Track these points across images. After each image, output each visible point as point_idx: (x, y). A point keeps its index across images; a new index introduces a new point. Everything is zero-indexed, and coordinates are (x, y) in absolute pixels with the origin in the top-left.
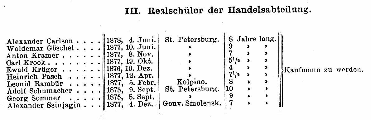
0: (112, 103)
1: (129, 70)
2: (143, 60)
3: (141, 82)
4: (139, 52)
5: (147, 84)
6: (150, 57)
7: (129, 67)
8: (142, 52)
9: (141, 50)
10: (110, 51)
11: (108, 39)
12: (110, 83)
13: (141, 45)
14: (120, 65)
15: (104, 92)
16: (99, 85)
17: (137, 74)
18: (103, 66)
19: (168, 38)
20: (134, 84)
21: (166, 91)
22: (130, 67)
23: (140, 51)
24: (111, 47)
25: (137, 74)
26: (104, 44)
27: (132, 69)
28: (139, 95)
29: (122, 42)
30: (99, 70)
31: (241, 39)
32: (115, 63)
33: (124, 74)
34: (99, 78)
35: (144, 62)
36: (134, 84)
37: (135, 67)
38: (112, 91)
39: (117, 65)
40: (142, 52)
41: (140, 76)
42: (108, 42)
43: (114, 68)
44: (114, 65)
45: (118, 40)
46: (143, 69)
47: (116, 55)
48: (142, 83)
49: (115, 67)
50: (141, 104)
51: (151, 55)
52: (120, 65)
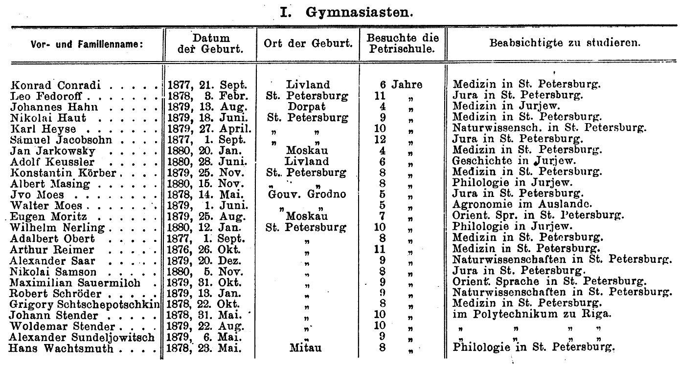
0: (175, 259)
1: (205, 295)
2: (227, 280)
3: (224, 95)
4: (222, 169)
5: (235, 98)
6: (239, 277)
7: (206, 104)
8: (226, 169)
9: (225, 166)
10: (172, 244)
11: (170, 82)
12: (171, 250)
13: (225, 115)
14: (189, 144)
15: (162, 265)
16: (156, 164)
17: (215, 324)
18: (162, 278)
19: (271, 169)
20: (212, 219)
21: (268, 120)
22: (208, 104)
23: (223, 167)
24: (174, 173)
25: (215, 324)
26: (163, 200)
27: (210, 108)
28: (221, 236)
29: (192, 99)
30: (155, 351)
31: (398, 85)
32: (181, 142)
33: (195, 226)
34: (155, 285)
35: (229, 284)
36: (211, 275)
37: (213, 301)
38: (175, 339)
39: (184, 243)
40: (226, 169)
41: (222, 129)
42: (170, 219)
43: (179, 249)
44: (178, 243)
45: (186, 96)
46: (228, 262)
47: (181, 239)
48: (226, 96)
49: (180, 247)
51: (240, 273)
52: (189, 90)
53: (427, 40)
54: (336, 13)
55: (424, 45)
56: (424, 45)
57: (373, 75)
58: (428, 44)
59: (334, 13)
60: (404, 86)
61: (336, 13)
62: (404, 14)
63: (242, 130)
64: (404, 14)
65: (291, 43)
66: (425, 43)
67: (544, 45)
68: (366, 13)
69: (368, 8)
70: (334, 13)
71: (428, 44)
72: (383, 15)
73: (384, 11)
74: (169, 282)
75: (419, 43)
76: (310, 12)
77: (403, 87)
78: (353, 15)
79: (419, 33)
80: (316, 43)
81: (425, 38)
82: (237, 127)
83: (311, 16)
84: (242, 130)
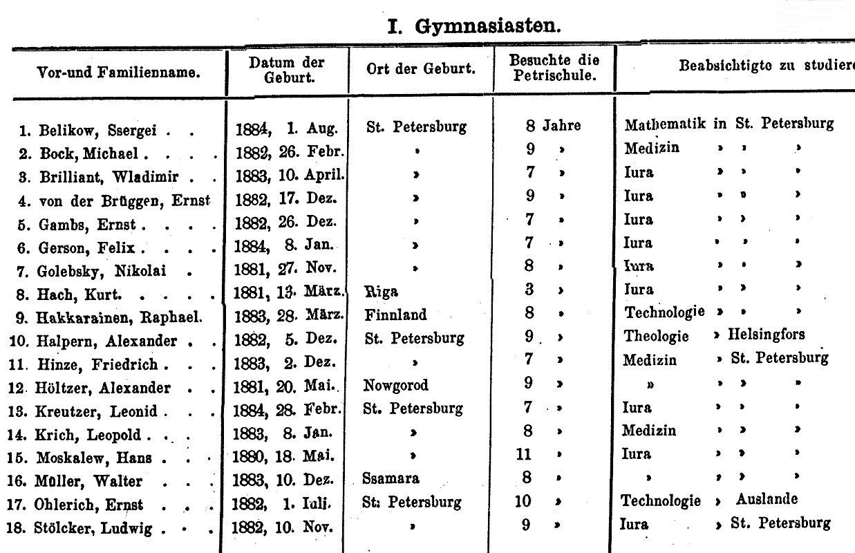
50: (313, 199)
53: (584, 64)
54: (457, 28)
55: (582, 70)
56: (582, 70)
57: (512, 112)
58: (587, 69)
59: (454, 28)
60: (559, 127)
61: (457, 28)
62: (550, 28)
63: (334, 176)
64: (550, 28)
65: (400, 70)
66: (582, 67)
67: (748, 69)
68: (498, 27)
69: (501, 19)
70: (454, 28)
71: (587, 69)
72: (520, 29)
73: (522, 23)
74: (237, 433)
75: (574, 68)
76: (423, 25)
77: (556, 130)
78: (482, 29)
79: (574, 53)
80: (430, 69)
81: (582, 60)
82: (327, 173)
83: (423, 33)
84: (334, 176)
